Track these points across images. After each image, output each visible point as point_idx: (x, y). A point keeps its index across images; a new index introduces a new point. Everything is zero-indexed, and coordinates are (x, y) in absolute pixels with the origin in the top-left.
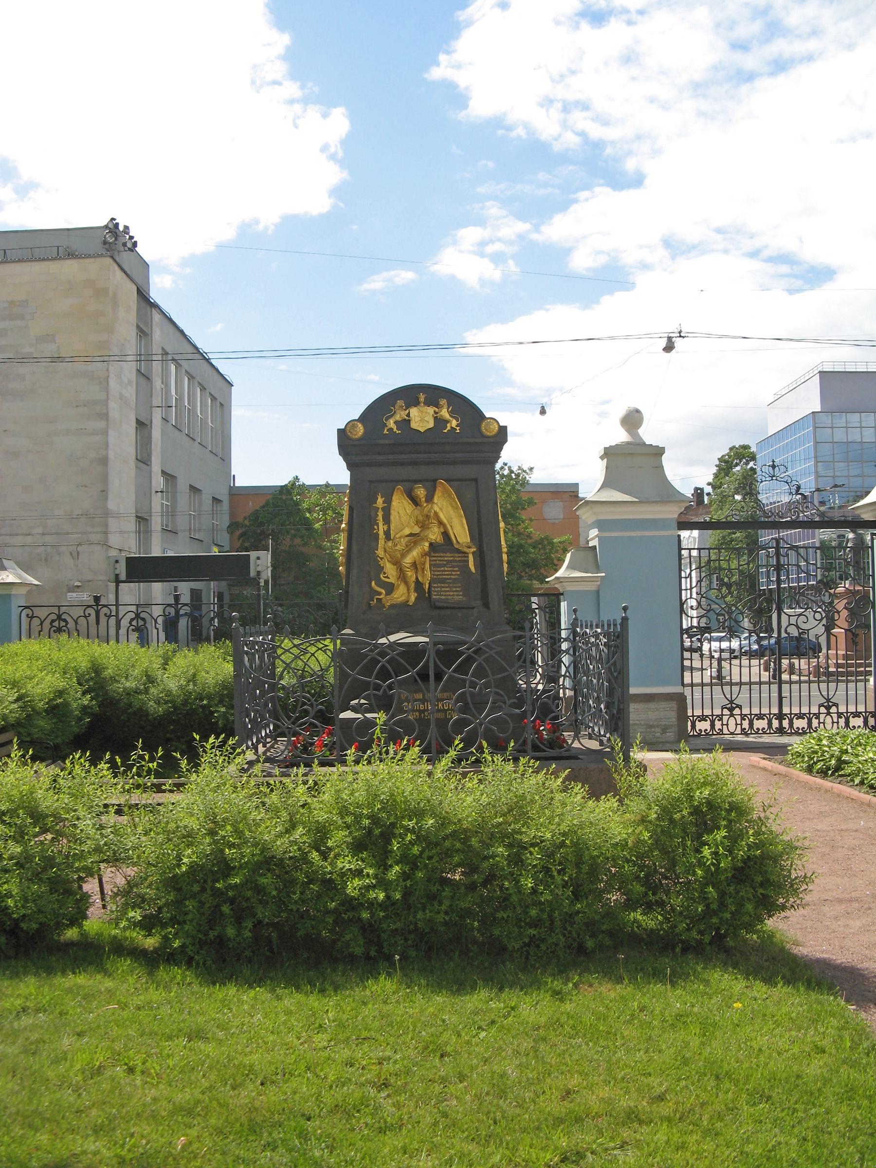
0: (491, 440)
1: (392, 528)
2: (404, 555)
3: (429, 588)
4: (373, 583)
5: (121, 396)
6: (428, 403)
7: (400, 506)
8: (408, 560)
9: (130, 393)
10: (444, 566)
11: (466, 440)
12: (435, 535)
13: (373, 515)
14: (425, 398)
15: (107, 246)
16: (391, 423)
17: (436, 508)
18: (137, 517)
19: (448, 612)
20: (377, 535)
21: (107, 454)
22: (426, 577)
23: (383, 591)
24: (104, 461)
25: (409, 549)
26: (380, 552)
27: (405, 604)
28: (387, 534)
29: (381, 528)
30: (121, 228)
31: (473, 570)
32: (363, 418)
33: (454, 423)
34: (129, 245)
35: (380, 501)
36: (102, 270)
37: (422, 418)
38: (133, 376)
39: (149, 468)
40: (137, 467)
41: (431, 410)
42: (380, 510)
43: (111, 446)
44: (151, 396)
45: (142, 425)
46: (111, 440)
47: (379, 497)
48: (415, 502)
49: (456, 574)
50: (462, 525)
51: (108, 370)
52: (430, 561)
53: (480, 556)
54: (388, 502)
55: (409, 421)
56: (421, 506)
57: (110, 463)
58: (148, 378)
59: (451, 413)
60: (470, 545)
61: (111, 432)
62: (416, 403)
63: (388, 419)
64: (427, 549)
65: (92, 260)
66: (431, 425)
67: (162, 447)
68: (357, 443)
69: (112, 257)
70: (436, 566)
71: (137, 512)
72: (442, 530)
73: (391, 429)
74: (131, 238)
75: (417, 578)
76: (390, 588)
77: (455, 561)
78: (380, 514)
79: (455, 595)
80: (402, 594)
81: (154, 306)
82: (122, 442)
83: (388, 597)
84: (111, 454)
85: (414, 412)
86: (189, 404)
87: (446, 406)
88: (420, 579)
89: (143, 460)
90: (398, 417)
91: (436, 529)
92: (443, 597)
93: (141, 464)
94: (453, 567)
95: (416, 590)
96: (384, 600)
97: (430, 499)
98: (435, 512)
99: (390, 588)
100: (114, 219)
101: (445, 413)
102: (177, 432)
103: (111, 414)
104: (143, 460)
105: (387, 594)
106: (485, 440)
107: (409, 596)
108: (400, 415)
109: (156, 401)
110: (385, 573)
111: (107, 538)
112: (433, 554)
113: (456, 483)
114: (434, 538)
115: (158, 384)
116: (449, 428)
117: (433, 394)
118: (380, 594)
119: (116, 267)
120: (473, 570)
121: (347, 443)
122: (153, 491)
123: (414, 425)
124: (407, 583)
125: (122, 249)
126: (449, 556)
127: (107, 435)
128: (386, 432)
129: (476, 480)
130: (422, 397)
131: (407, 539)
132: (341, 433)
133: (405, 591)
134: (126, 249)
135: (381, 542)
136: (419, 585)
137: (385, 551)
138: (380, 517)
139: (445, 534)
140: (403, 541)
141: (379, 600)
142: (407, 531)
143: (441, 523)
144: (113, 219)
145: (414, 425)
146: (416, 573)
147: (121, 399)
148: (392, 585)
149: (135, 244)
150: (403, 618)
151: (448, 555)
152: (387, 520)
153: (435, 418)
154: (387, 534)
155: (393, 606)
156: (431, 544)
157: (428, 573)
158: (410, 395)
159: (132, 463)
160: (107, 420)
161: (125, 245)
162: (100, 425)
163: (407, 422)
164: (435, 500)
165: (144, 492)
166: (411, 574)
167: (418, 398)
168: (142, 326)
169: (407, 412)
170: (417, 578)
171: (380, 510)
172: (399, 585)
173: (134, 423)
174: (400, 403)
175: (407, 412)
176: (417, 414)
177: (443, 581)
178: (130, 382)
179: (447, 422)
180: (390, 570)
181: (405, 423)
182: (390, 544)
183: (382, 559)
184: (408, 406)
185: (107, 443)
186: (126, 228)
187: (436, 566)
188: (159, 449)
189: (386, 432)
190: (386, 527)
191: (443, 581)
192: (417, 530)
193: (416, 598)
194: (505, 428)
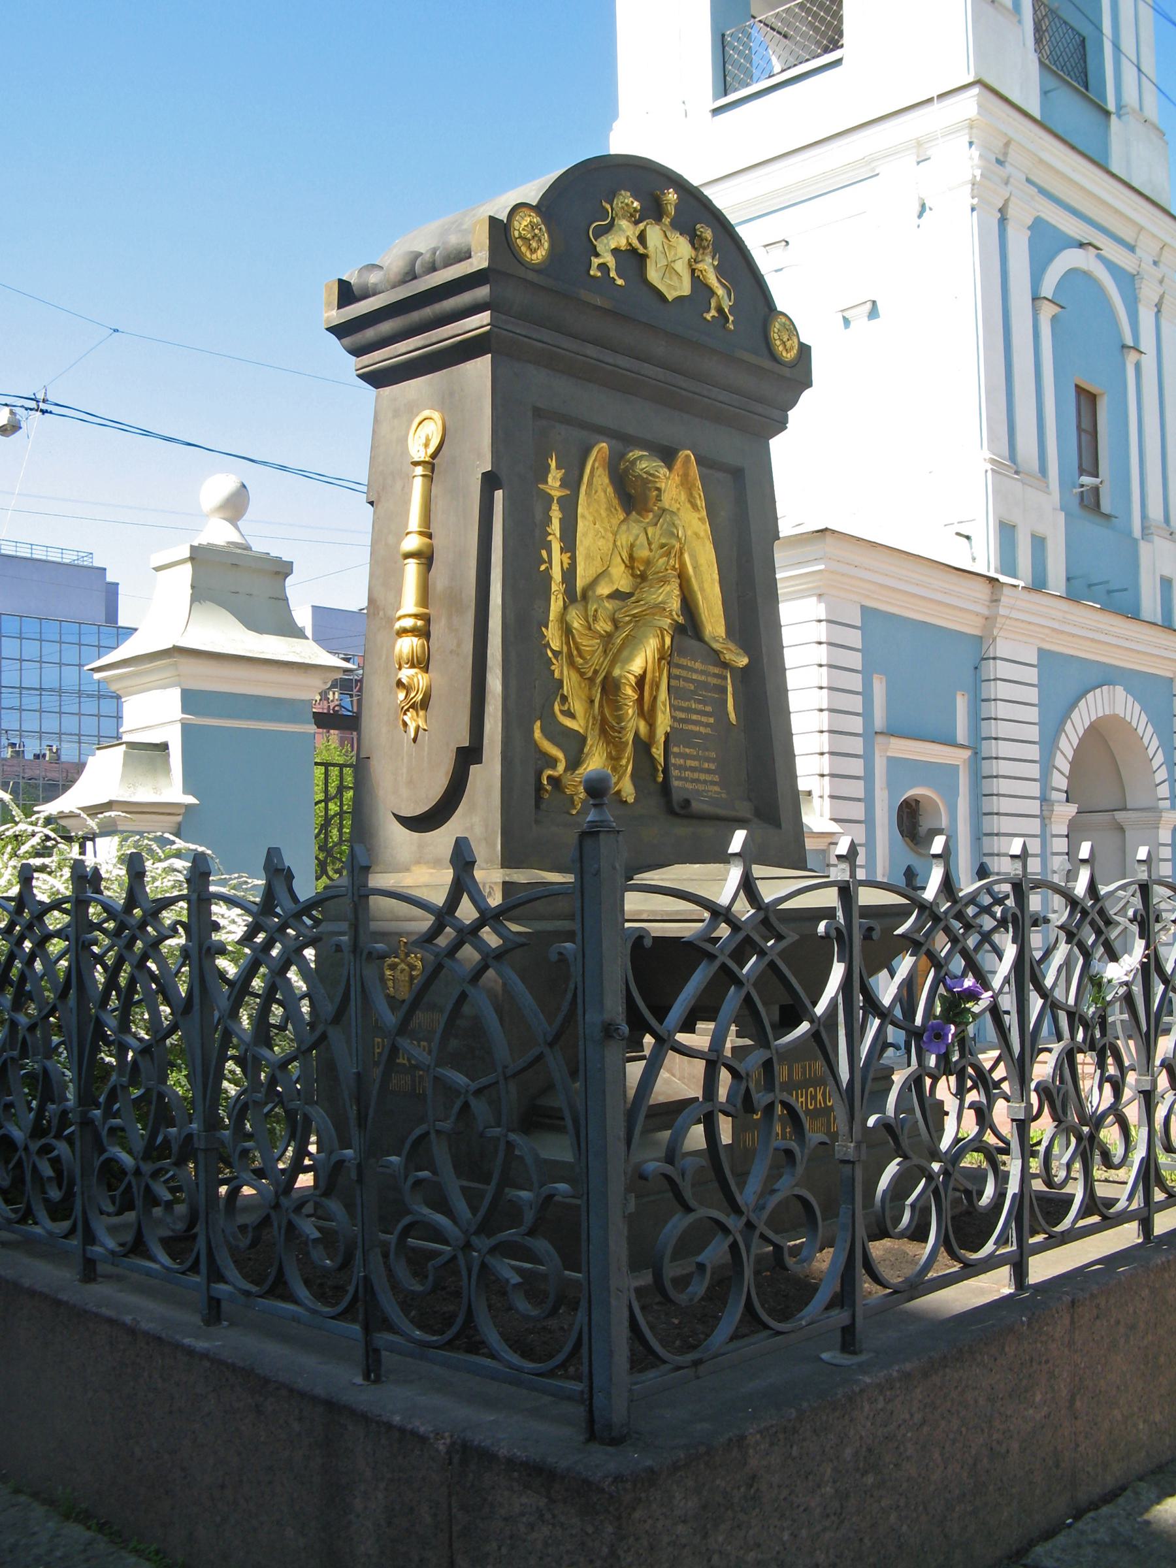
13: (539, 516)
23: (559, 755)
29: (558, 560)
31: (732, 716)
37: (672, 263)
42: (555, 507)
54: (572, 483)
55: (643, 258)
68: (531, 276)
78: (556, 514)
94: (704, 703)
108: (624, 235)
118: (552, 762)
120: (732, 716)
171: (555, 507)
181: (634, 259)
190: (566, 561)
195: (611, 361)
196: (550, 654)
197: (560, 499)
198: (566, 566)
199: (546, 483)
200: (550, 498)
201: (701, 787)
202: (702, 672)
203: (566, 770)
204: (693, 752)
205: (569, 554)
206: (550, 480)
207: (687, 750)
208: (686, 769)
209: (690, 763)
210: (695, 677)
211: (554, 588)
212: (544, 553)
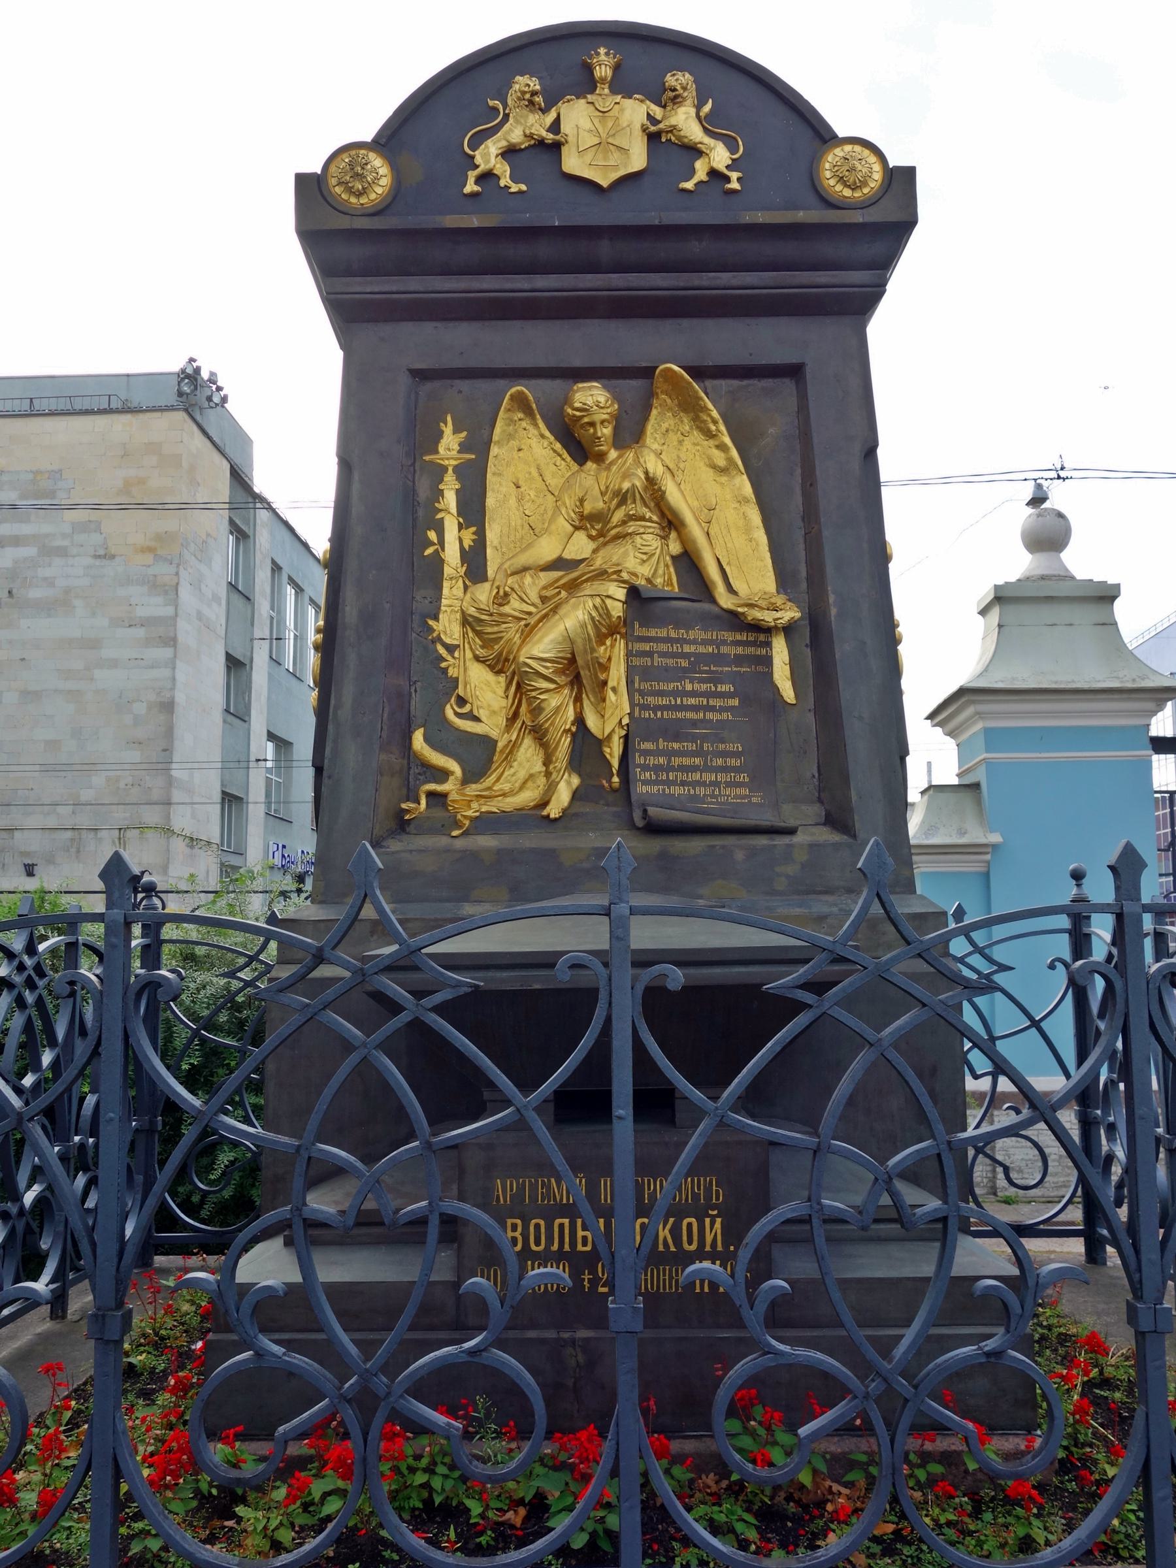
0: (858, 217)
1: (492, 536)
2: (528, 632)
3: (625, 758)
4: (418, 740)
5: (200, 616)
6: (622, 85)
7: (524, 456)
8: (543, 647)
9: (217, 614)
10: (680, 674)
11: (761, 217)
12: (644, 559)
13: (423, 492)
14: (617, 68)
15: (184, 399)
16: (489, 155)
17: (654, 466)
18: (223, 793)
19: (695, 845)
20: (438, 562)
21: (173, 698)
22: (610, 718)
24: (168, 707)
25: (550, 607)
26: (448, 627)
27: (534, 817)
28: (475, 564)
29: (453, 540)
30: (205, 375)
32: (394, 137)
33: (720, 156)
34: (216, 399)
35: (450, 445)
36: (174, 430)
37: (602, 139)
38: (223, 591)
39: (246, 725)
40: (225, 721)
41: (635, 112)
43: (179, 685)
44: (252, 625)
45: (235, 665)
46: (180, 677)
47: (448, 430)
48: (577, 444)
49: (725, 705)
50: (748, 529)
51: (177, 574)
52: (629, 654)
53: (815, 637)
54: (478, 446)
55: (557, 147)
56: (600, 458)
57: (178, 710)
58: (248, 599)
59: (709, 124)
60: (779, 600)
61: (179, 664)
62: (586, 84)
63: (478, 140)
64: (617, 610)
65: (159, 414)
66: (638, 160)
67: (269, 698)
69: (186, 410)
70: (647, 674)
71: (222, 785)
72: (675, 548)
73: (488, 177)
74: (219, 389)
75: (580, 721)
76: (480, 756)
77: (718, 659)
79: (724, 792)
80: (528, 779)
81: (258, 498)
82: (202, 684)
83: (473, 789)
84: (180, 697)
85: (577, 117)
86: (296, 628)
87: (691, 95)
88: (592, 722)
89: (237, 711)
90: (514, 133)
91: (651, 540)
92: (677, 791)
93: (230, 718)
94: (716, 681)
95: (576, 763)
96: (453, 796)
97: (630, 432)
98: (650, 480)
99: (480, 756)
100: (194, 361)
101: (686, 121)
102: (294, 680)
103: (181, 638)
104: (237, 711)
105: (470, 777)
106: (832, 216)
107: (551, 788)
108: (522, 127)
109: (262, 630)
110: (462, 701)
111: (168, 817)
112: (639, 631)
113: (724, 384)
114: (645, 571)
115: (263, 607)
116: (701, 174)
117: (649, 55)
118: (442, 775)
119: (195, 428)
121: (326, 216)
122: (253, 758)
123: (572, 163)
124: (539, 734)
125: (206, 404)
126: (699, 640)
127: (174, 668)
128: (471, 187)
129: (794, 372)
130: (603, 64)
131: (546, 577)
132: (309, 189)
133: (539, 767)
134: (212, 404)
135: (452, 593)
136: (585, 745)
137: (466, 621)
138: (450, 499)
139: (688, 562)
140: (533, 585)
141: (437, 798)
142: (547, 550)
143: (671, 522)
144: (192, 360)
145: (572, 163)
146: (578, 700)
147: (200, 619)
148: (488, 743)
149: (224, 399)
150: (526, 860)
151: (696, 634)
152: (473, 511)
153: (653, 138)
154: (475, 564)
155: (486, 823)
156: (634, 592)
157: (619, 704)
158: (559, 56)
159: (217, 715)
160: (175, 646)
161: (209, 399)
162: (167, 653)
163: (549, 149)
164: (649, 440)
165: (237, 760)
166: (559, 706)
167: (589, 69)
168: (238, 522)
169: (552, 115)
170: (580, 721)
172: (514, 746)
173: (222, 659)
174: (525, 83)
175: (552, 115)
176: (586, 124)
177: (674, 731)
178: (216, 598)
179: (695, 151)
180: (486, 692)
182: (483, 593)
183: (451, 649)
184: (552, 98)
185: (174, 679)
186: (213, 379)
187: (647, 674)
188: (264, 699)
189: (471, 187)
190: (468, 537)
191: (674, 731)
192: (580, 546)
193: (576, 795)
194: (909, 174)
195: (526, 286)
196: (442, 651)
197: (456, 469)
198: (467, 543)
199: (437, 452)
200: (444, 469)
201: (701, 791)
202: (705, 642)
203: (466, 781)
204: (691, 746)
205: (474, 529)
206: (441, 450)
207: (676, 746)
208: (670, 768)
209: (676, 761)
210: (687, 649)
211: (448, 571)
212: (432, 535)
